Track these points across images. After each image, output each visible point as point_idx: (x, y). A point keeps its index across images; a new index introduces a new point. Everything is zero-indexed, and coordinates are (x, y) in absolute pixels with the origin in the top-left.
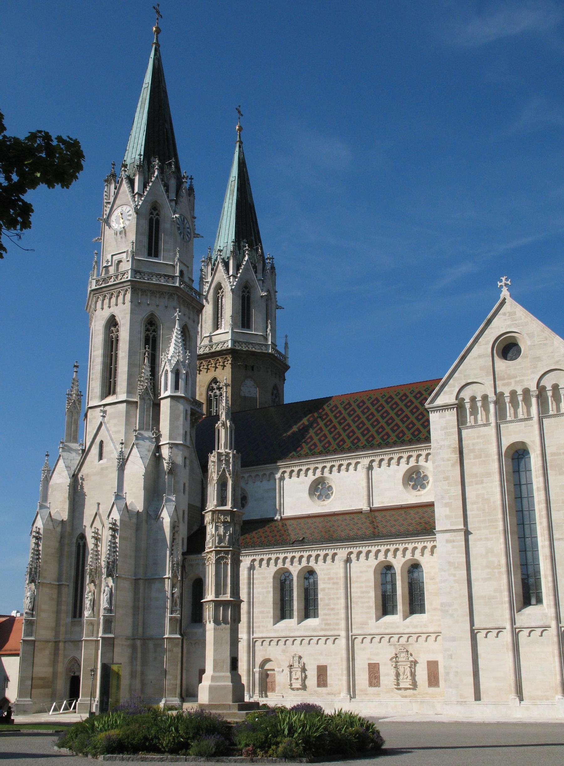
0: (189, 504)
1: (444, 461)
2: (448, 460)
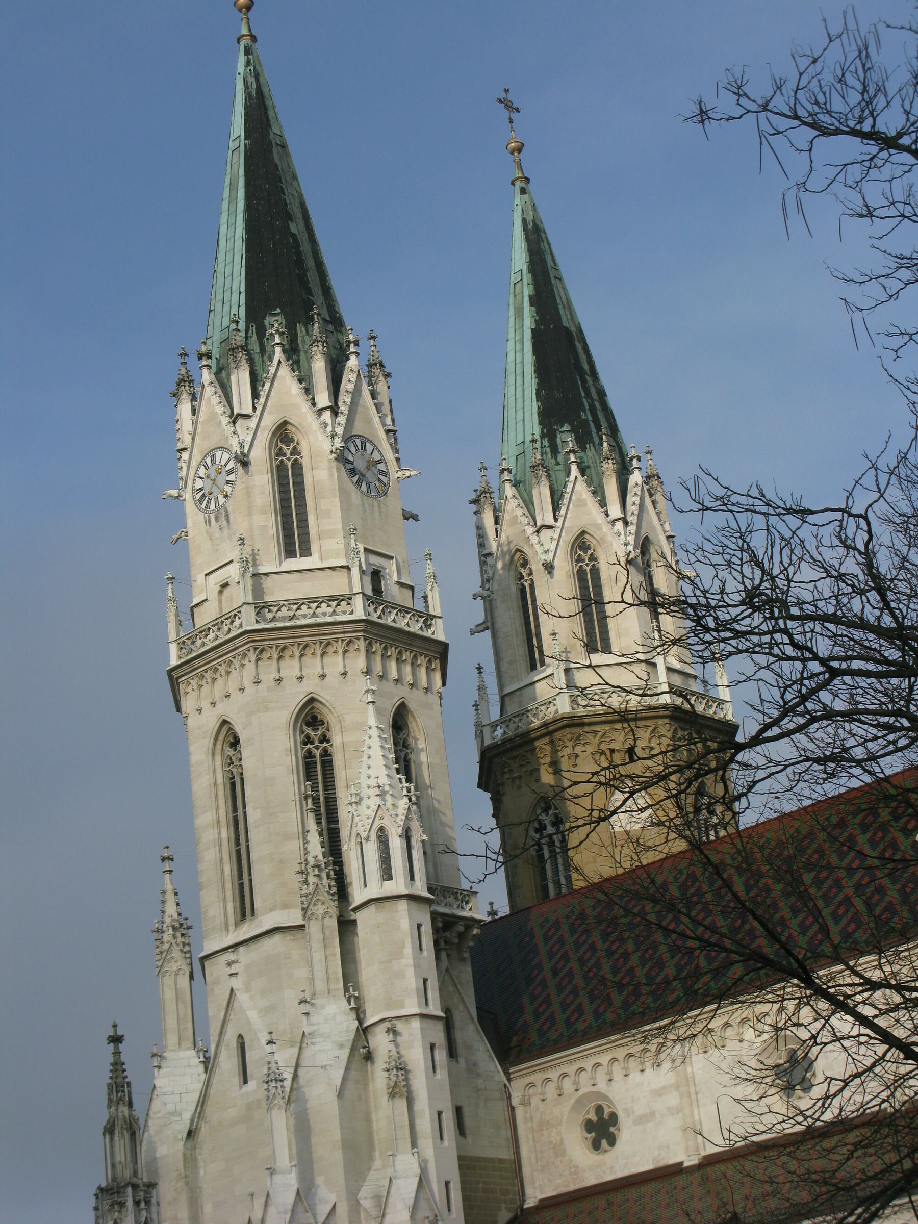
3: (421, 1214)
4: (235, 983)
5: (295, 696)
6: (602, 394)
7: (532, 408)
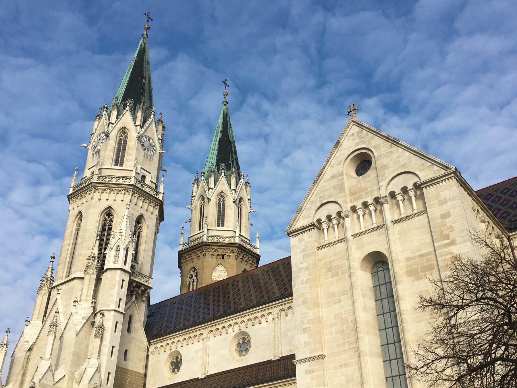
0: (117, 367)
1: (303, 284)
2: (306, 283)
3: (93, 382)
4: (59, 297)
5: (104, 205)
6: (237, 159)
7: (215, 158)
